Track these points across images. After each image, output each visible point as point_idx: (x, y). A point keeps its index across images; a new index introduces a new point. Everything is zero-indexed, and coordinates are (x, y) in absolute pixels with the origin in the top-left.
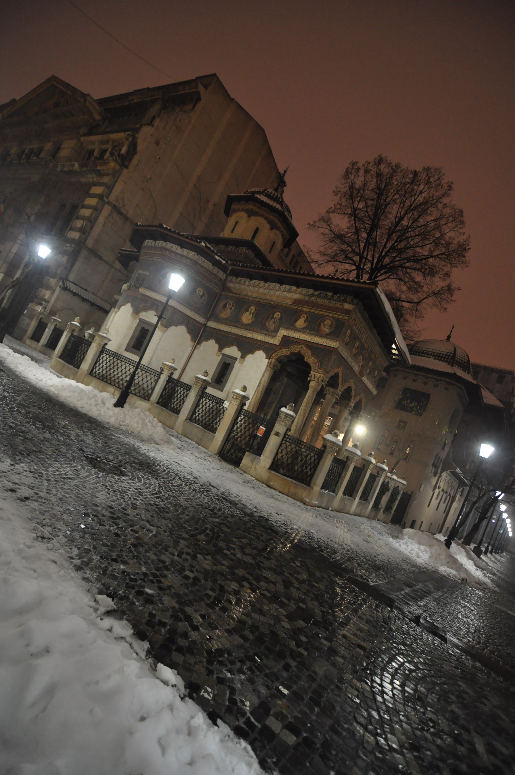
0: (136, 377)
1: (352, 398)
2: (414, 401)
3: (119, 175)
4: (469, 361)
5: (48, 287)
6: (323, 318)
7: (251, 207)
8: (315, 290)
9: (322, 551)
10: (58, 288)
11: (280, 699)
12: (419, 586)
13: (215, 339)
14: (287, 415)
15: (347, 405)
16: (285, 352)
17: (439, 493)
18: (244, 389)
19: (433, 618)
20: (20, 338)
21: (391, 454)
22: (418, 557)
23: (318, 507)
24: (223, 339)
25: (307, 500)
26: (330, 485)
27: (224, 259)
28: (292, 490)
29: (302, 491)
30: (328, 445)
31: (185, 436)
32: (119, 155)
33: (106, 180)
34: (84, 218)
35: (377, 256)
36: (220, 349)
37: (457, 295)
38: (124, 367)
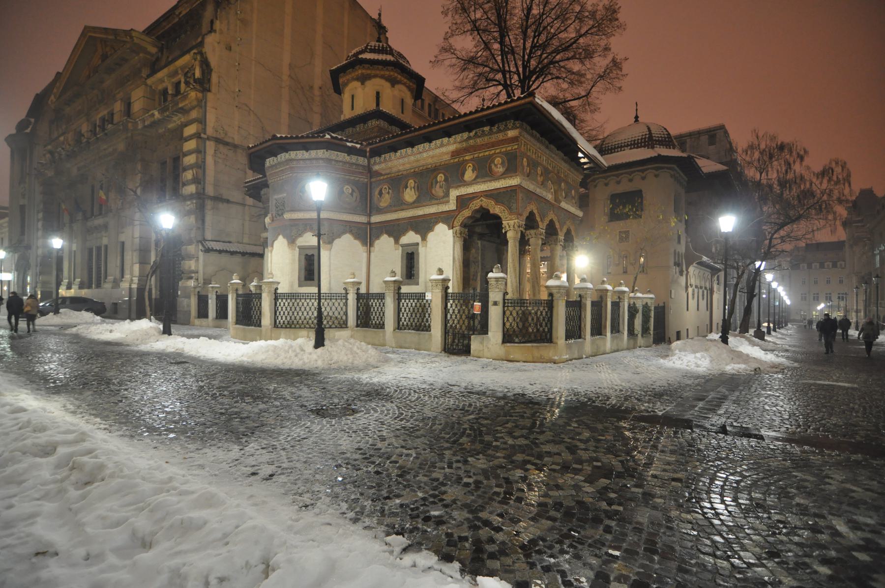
0: (323, 309)
2: (627, 204)
3: (206, 103)
4: (669, 134)
5: (190, 257)
6: (490, 159)
7: (360, 72)
8: (470, 131)
9: (594, 402)
10: (201, 254)
11: (615, 562)
12: (712, 395)
13: (386, 233)
14: (497, 279)
15: (556, 241)
16: (467, 213)
17: (693, 291)
18: (440, 271)
19: (740, 420)
20: (187, 322)
21: (625, 272)
22: (698, 366)
23: (571, 360)
24: (395, 230)
25: (556, 358)
26: (574, 332)
27: (357, 143)
28: (537, 354)
29: (545, 350)
30: (554, 291)
31: (401, 347)
32: (195, 81)
33: (194, 114)
34: (191, 167)
35: (520, 63)
37: (626, 67)
38: (305, 304)
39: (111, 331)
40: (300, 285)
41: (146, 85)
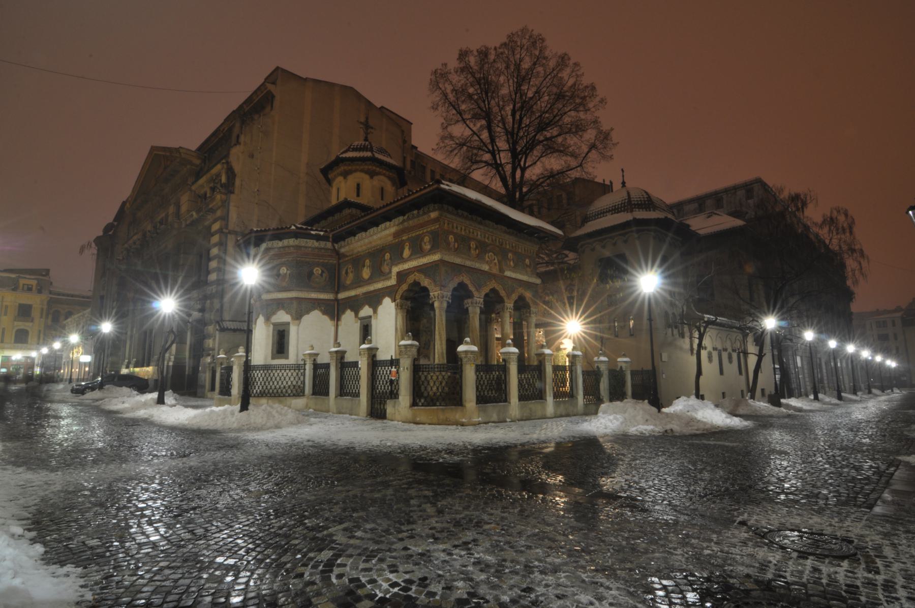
1: (505, 298)
4: (649, 197)
5: (209, 336)
6: (420, 238)
8: (404, 215)
14: (406, 346)
16: (405, 287)
20: (203, 396)
21: (617, 336)
23: (486, 423)
24: (355, 305)
28: (442, 417)
29: (457, 415)
31: (340, 413)
32: (222, 186)
37: (615, 136)
39: (123, 403)
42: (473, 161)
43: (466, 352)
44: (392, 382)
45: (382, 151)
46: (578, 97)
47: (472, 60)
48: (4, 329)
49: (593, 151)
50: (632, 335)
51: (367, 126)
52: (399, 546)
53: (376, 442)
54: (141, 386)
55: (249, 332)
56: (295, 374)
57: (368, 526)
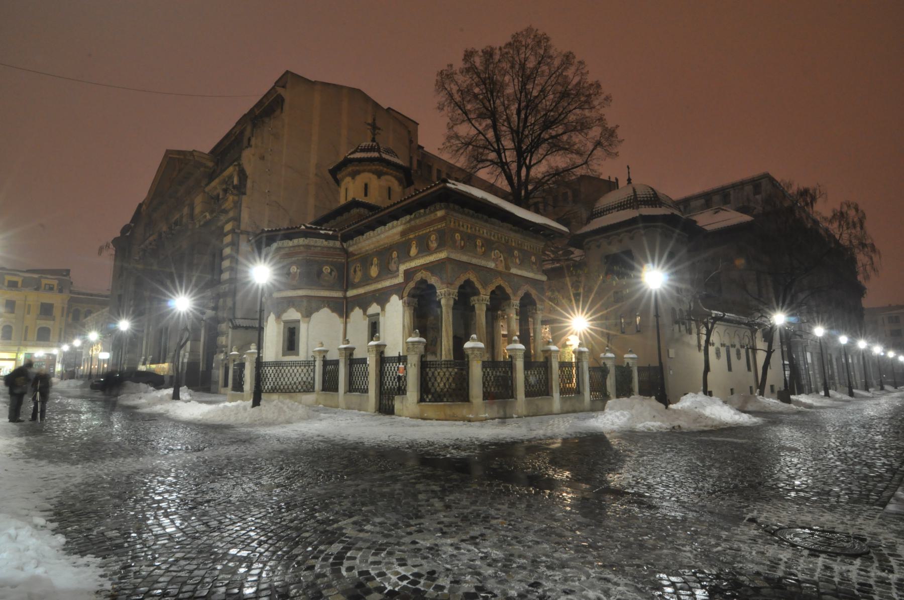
4: (655, 194)
5: (222, 334)
6: (427, 237)
14: (413, 343)
16: (412, 285)
20: (216, 392)
21: (623, 333)
25: (470, 416)
29: (462, 410)
30: (470, 352)
31: (349, 408)
32: (234, 187)
33: (231, 214)
36: (365, 312)
37: (619, 133)
39: (140, 398)
40: (284, 355)
41: (204, 192)
42: (478, 160)
43: (473, 349)
44: (399, 378)
45: (389, 151)
46: (585, 94)
47: (478, 61)
48: (27, 327)
49: (599, 149)
50: (638, 331)
51: (374, 127)
52: (407, 540)
53: (384, 437)
54: (157, 381)
55: (261, 330)
56: (305, 370)
57: (377, 520)
